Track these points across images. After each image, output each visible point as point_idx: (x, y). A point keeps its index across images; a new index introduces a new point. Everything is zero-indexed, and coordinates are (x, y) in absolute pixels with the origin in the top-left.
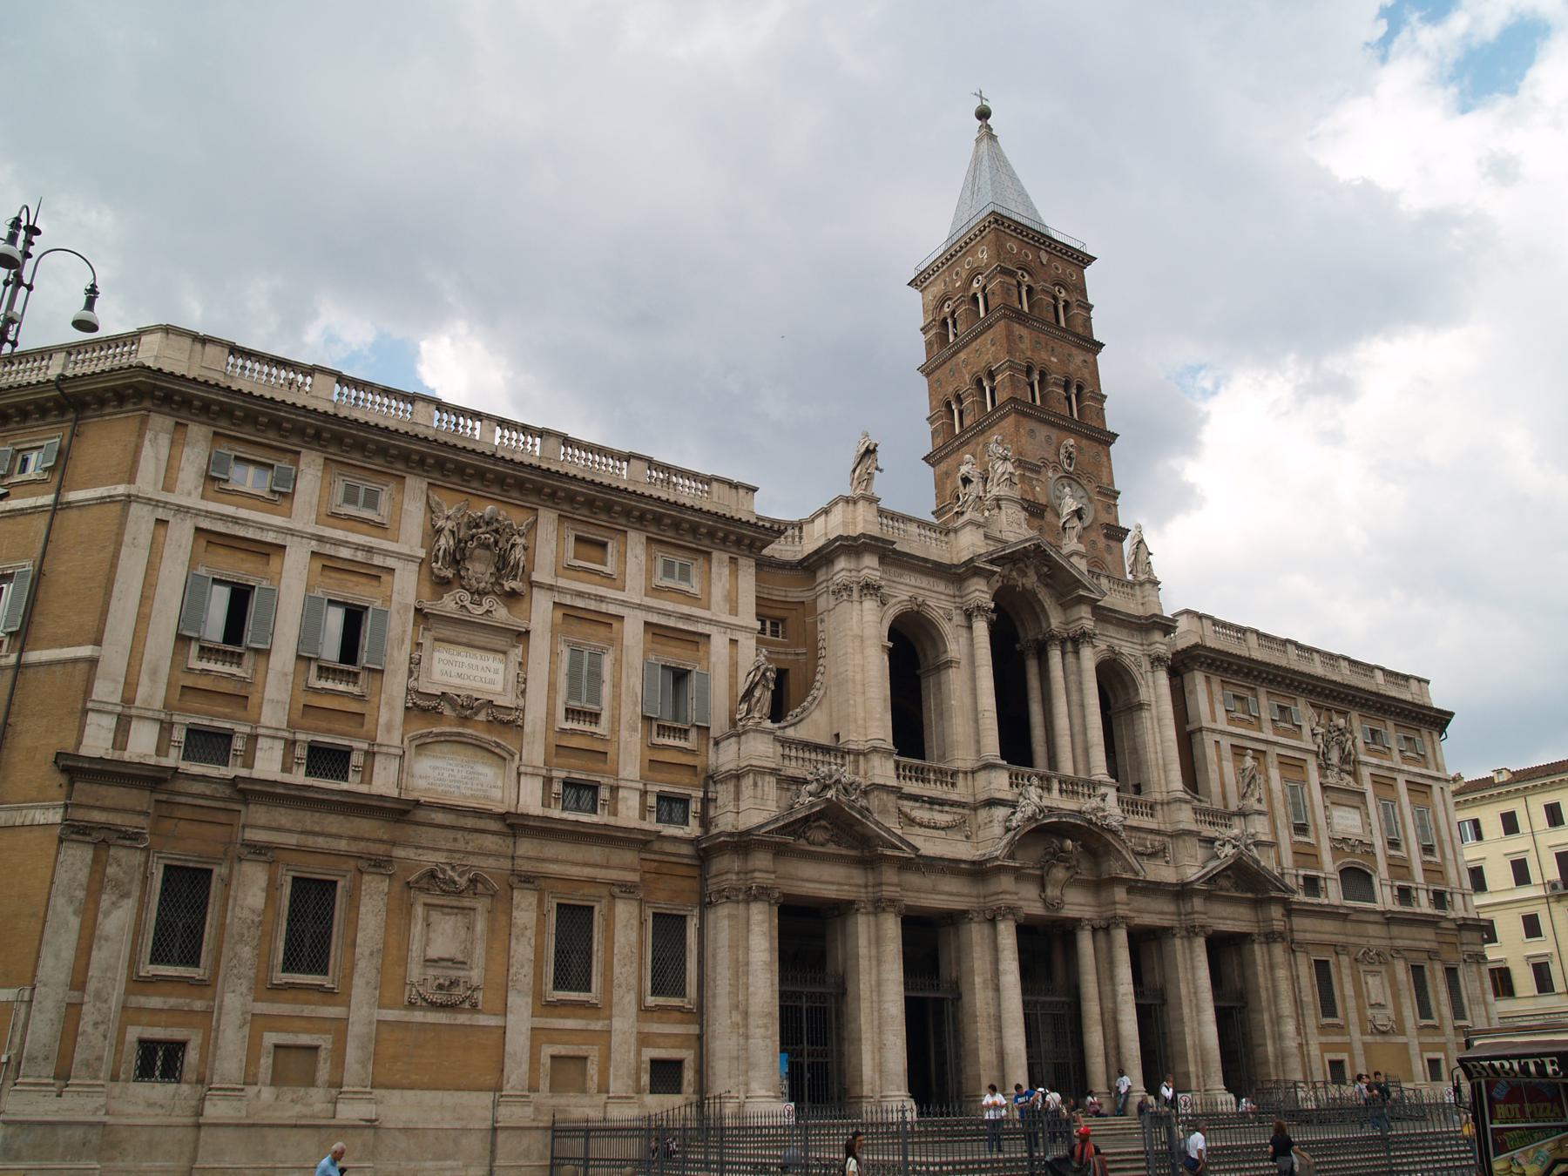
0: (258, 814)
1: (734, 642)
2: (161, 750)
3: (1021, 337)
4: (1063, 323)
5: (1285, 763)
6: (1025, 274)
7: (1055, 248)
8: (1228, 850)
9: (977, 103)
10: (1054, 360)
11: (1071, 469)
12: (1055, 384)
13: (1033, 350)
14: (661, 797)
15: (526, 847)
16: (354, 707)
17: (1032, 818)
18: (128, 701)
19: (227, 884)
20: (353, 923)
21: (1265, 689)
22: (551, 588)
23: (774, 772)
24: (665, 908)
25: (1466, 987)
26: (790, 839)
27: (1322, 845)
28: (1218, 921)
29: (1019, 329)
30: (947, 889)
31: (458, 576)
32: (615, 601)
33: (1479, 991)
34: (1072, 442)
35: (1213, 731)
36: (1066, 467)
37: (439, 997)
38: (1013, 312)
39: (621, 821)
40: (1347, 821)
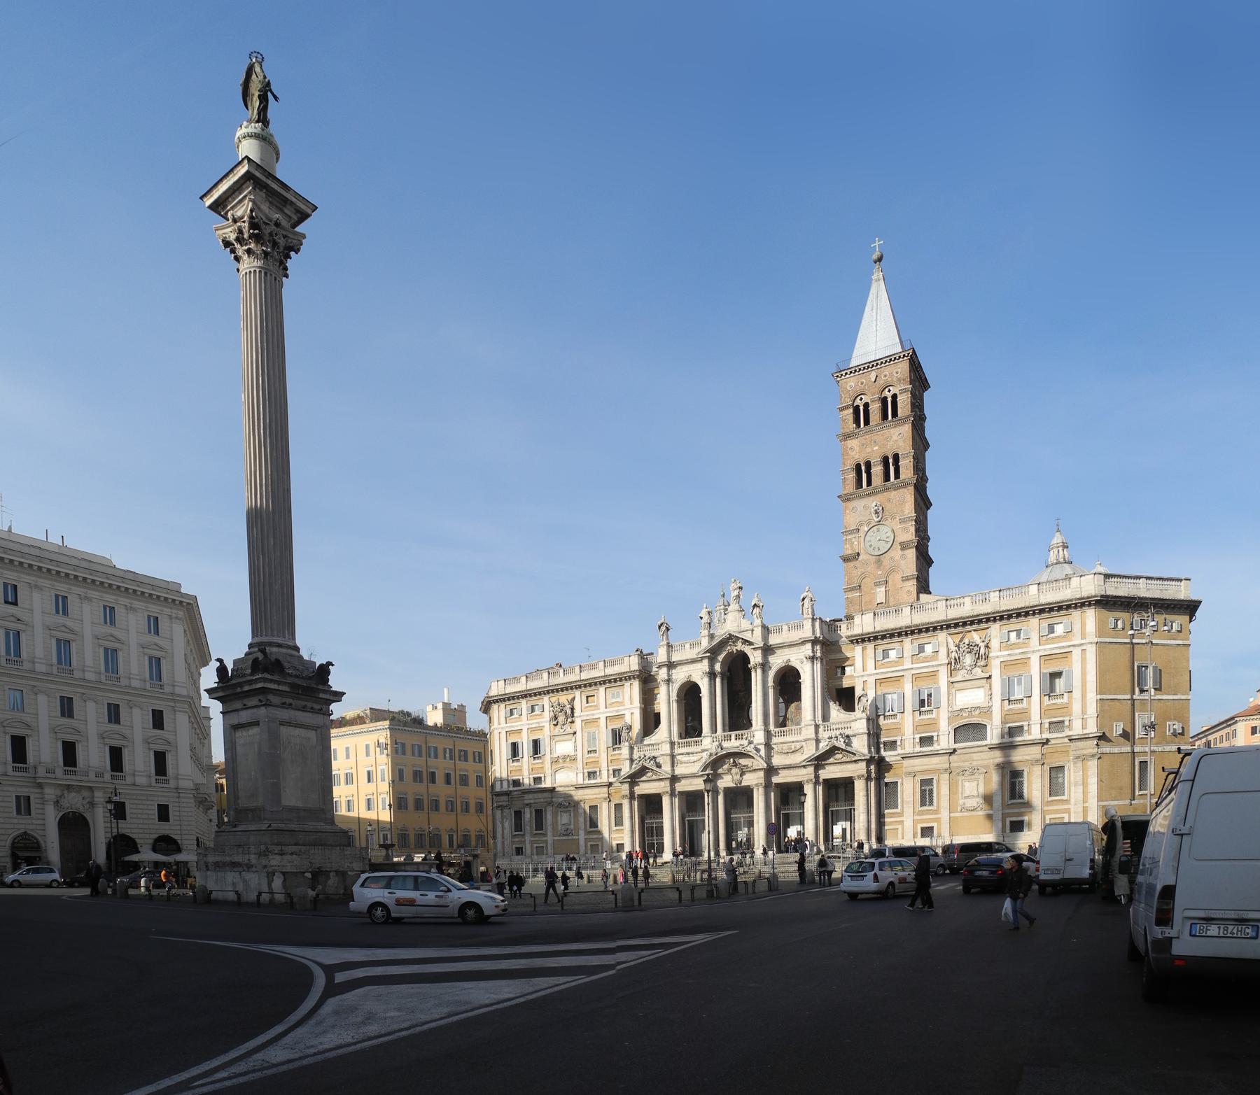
0: (526, 796)
2: (509, 787)
5: (916, 678)
8: (827, 743)
11: (878, 520)
14: (614, 771)
16: (541, 766)
17: (711, 755)
19: (524, 813)
20: (546, 818)
23: (627, 759)
24: (617, 802)
25: (1069, 777)
26: (629, 780)
27: (941, 717)
30: (695, 783)
33: (1079, 778)
35: (863, 676)
37: (565, 833)
39: (601, 781)
40: (971, 697)
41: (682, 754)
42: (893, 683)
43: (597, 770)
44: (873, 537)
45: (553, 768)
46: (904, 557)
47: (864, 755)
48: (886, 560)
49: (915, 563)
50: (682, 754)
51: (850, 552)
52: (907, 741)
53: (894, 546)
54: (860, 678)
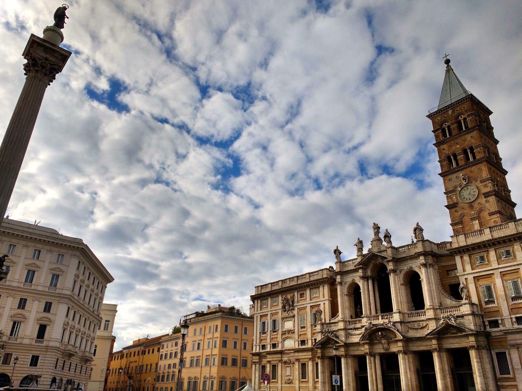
1: (324, 304)
3: (443, 149)
4: (464, 129)
6: (446, 123)
7: (454, 105)
9: (445, 59)
10: (457, 147)
12: (459, 155)
13: (448, 150)
15: (296, 354)
17: (366, 329)
18: (256, 343)
21: (493, 249)
22: (297, 306)
26: (320, 346)
28: (451, 345)
29: (442, 147)
31: (286, 309)
32: (305, 304)
34: (461, 175)
35: (464, 275)
36: (465, 183)
37: (288, 382)
38: (437, 144)
41: (351, 329)
42: (487, 279)
43: (306, 339)
44: (465, 193)
45: (283, 337)
46: (487, 201)
47: (471, 330)
48: (476, 205)
49: (496, 204)
50: (351, 329)
51: (451, 203)
52: (506, 321)
53: (480, 196)
54: (462, 277)
